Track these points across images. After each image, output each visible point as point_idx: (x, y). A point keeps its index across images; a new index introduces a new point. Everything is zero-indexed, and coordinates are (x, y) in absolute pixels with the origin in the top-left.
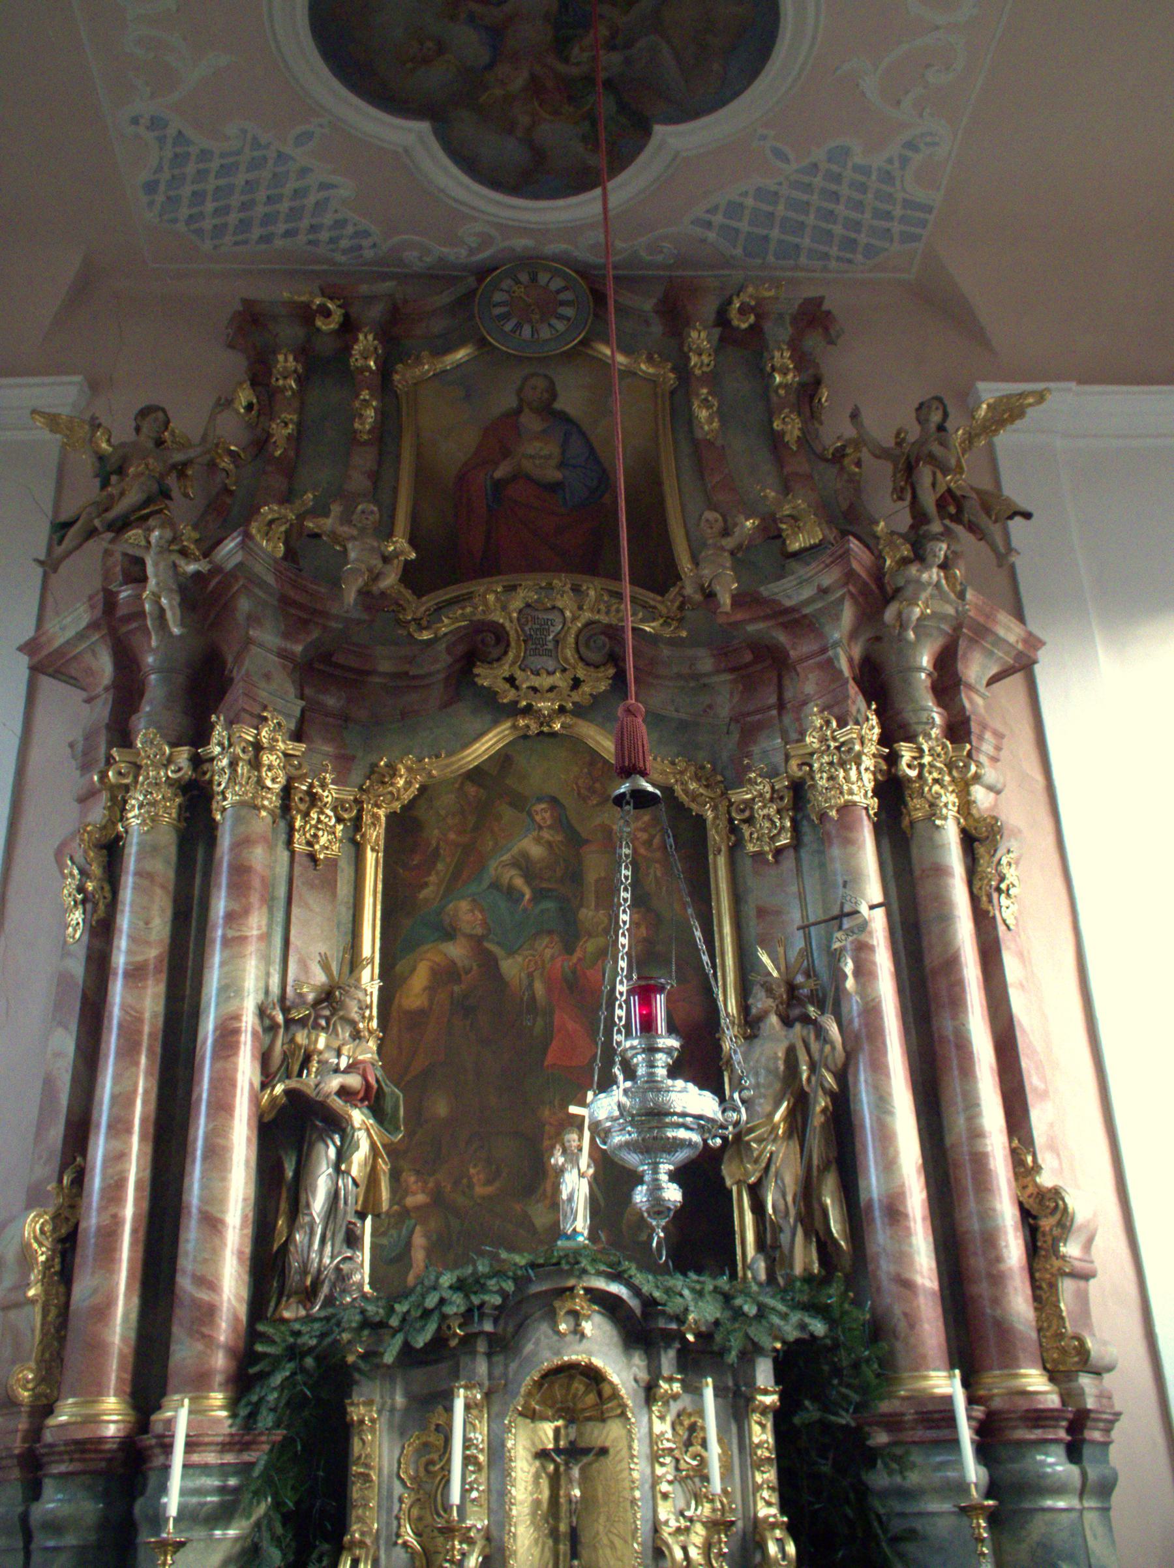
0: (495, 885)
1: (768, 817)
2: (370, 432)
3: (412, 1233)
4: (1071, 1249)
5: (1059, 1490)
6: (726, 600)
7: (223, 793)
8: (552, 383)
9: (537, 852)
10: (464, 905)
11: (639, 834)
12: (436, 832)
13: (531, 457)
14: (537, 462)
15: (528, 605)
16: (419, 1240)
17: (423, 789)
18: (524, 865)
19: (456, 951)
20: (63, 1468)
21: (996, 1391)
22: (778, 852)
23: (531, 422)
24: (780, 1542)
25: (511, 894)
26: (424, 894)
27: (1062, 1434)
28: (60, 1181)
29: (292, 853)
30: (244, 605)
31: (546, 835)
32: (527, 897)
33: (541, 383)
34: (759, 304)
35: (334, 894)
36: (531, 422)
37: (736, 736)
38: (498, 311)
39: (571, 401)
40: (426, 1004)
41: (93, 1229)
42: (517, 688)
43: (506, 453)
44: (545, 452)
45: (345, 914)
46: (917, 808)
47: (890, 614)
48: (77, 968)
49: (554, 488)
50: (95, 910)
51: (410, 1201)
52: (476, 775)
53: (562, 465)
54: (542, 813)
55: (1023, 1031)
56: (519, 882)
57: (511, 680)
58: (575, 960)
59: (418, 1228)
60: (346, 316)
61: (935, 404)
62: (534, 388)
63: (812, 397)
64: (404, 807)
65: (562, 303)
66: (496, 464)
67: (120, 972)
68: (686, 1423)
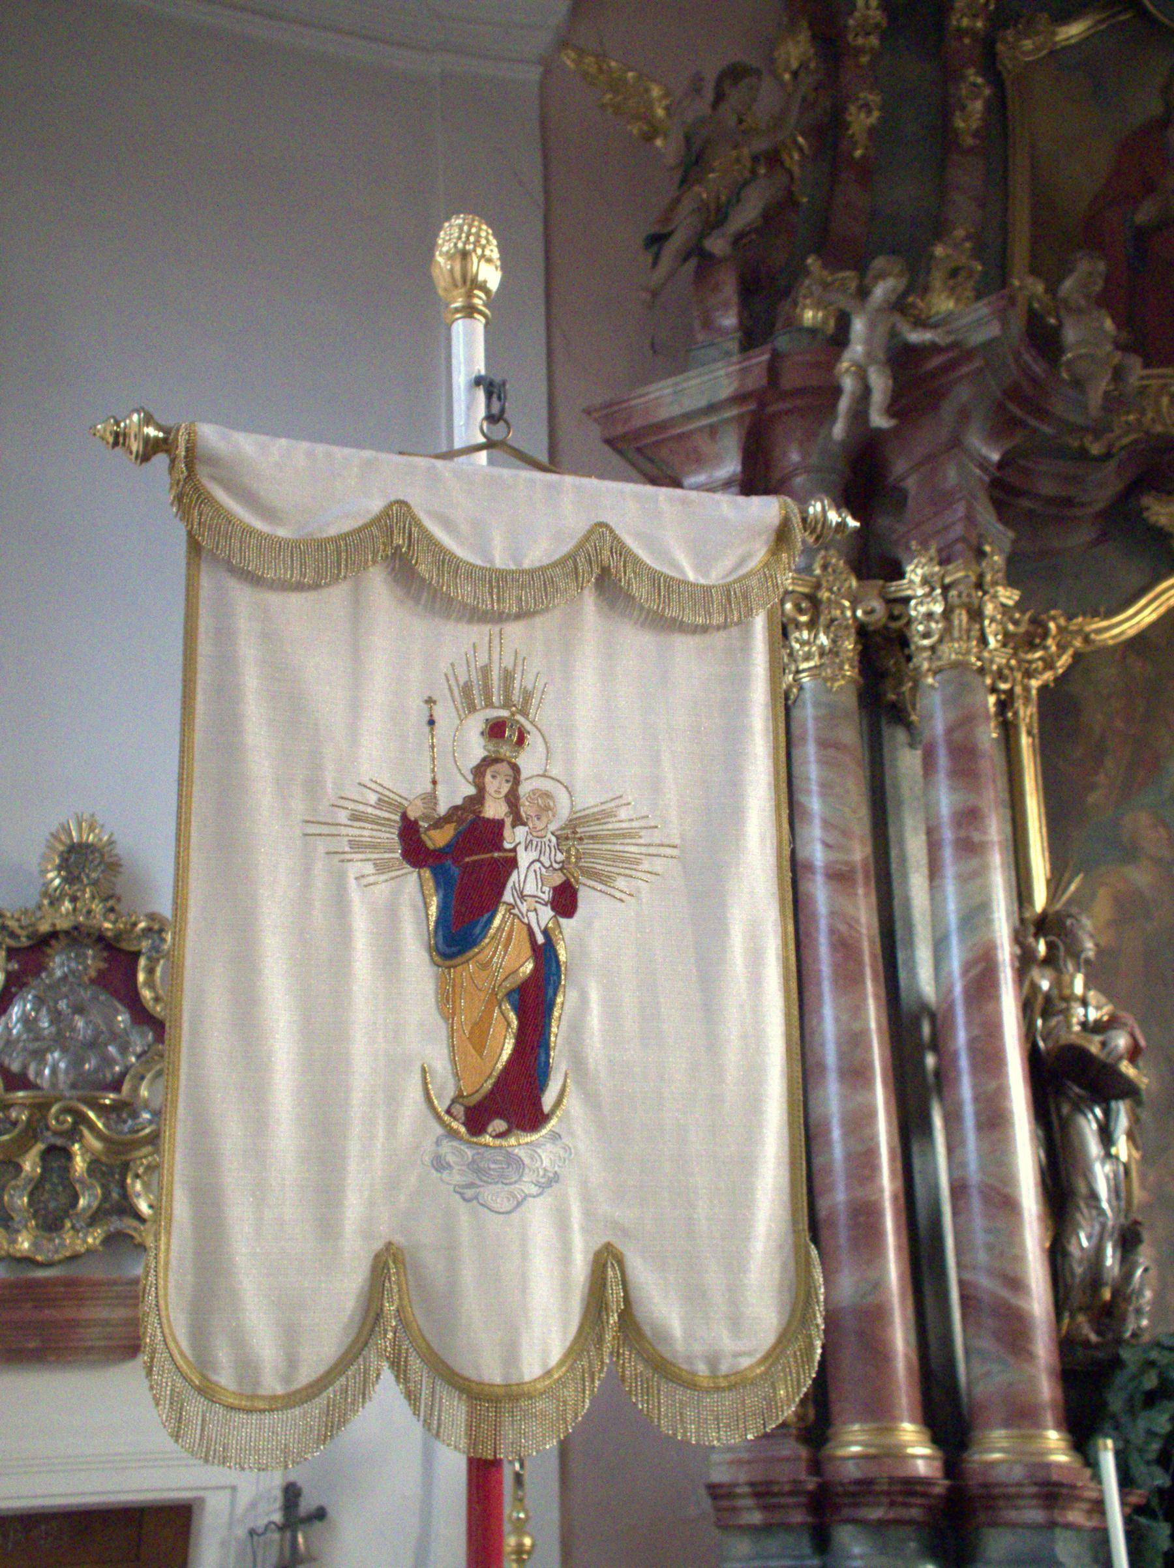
2: (975, 135)
10: (1144, 818)
12: (1099, 717)
20: (876, 1514)
26: (1092, 798)
30: (963, 393)
41: (841, 1208)
43: (1149, 187)
64: (1057, 680)
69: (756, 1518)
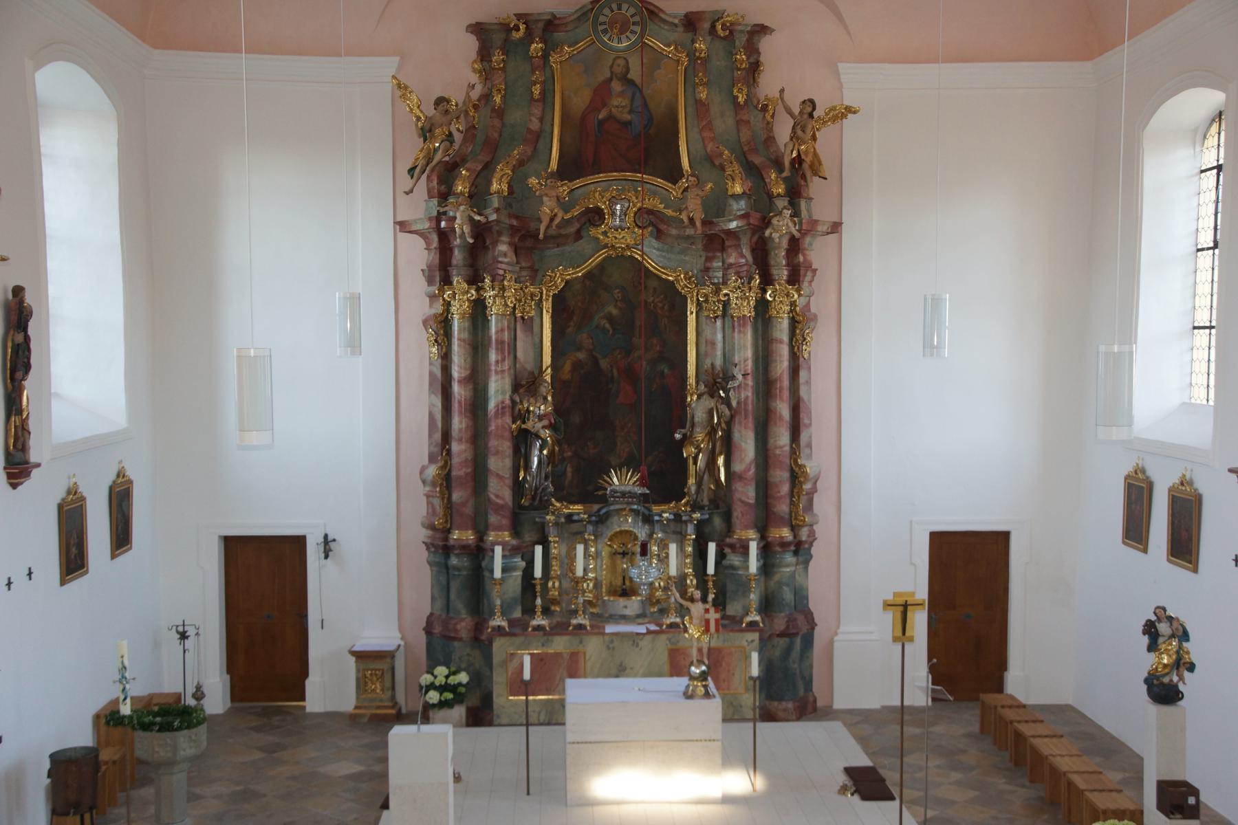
0: (597, 327)
1: (714, 302)
3: (566, 466)
4: (807, 486)
5: (788, 566)
6: (698, 224)
9: (615, 312)
10: (585, 336)
11: (659, 304)
13: (617, 107)
14: (620, 109)
15: (613, 197)
16: (569, 469)
17: (567, 282)
18: (610, 318)
21: (771, 535)
23: (616, 86)
24: (691, 581)
26: (570, 330)
27: (793, 548)
28: (442, 455)
29: (516, 318)
31: (619, 304)
32: (611, 333)
34: (732, 24)
35: (532, 333)
36: (616, 86)
37: (703, 259)
38: (601, 28)
39: (634, 74)
40: (570, 378)
42: (608, 237)
43: (605, 105)
44: (624, 104)
45: (537, 340)
47: (767, 233)
48: (438, 372)
49: (627, 124)
50: (442, 349)
52: (589, 275)
53: (630, 112)
55: (803, 400)
56: (607, 326)
57: (605, 233)
58: (629, 360)
59: (569, 465)
60: (527, 28)
61: (809, 103)
62: (619, 66)
63: (754, 71)
65: (634, 24)
66: (599, 111)
67: (456, 380)
68: (663, 543)
69: (433, 549)
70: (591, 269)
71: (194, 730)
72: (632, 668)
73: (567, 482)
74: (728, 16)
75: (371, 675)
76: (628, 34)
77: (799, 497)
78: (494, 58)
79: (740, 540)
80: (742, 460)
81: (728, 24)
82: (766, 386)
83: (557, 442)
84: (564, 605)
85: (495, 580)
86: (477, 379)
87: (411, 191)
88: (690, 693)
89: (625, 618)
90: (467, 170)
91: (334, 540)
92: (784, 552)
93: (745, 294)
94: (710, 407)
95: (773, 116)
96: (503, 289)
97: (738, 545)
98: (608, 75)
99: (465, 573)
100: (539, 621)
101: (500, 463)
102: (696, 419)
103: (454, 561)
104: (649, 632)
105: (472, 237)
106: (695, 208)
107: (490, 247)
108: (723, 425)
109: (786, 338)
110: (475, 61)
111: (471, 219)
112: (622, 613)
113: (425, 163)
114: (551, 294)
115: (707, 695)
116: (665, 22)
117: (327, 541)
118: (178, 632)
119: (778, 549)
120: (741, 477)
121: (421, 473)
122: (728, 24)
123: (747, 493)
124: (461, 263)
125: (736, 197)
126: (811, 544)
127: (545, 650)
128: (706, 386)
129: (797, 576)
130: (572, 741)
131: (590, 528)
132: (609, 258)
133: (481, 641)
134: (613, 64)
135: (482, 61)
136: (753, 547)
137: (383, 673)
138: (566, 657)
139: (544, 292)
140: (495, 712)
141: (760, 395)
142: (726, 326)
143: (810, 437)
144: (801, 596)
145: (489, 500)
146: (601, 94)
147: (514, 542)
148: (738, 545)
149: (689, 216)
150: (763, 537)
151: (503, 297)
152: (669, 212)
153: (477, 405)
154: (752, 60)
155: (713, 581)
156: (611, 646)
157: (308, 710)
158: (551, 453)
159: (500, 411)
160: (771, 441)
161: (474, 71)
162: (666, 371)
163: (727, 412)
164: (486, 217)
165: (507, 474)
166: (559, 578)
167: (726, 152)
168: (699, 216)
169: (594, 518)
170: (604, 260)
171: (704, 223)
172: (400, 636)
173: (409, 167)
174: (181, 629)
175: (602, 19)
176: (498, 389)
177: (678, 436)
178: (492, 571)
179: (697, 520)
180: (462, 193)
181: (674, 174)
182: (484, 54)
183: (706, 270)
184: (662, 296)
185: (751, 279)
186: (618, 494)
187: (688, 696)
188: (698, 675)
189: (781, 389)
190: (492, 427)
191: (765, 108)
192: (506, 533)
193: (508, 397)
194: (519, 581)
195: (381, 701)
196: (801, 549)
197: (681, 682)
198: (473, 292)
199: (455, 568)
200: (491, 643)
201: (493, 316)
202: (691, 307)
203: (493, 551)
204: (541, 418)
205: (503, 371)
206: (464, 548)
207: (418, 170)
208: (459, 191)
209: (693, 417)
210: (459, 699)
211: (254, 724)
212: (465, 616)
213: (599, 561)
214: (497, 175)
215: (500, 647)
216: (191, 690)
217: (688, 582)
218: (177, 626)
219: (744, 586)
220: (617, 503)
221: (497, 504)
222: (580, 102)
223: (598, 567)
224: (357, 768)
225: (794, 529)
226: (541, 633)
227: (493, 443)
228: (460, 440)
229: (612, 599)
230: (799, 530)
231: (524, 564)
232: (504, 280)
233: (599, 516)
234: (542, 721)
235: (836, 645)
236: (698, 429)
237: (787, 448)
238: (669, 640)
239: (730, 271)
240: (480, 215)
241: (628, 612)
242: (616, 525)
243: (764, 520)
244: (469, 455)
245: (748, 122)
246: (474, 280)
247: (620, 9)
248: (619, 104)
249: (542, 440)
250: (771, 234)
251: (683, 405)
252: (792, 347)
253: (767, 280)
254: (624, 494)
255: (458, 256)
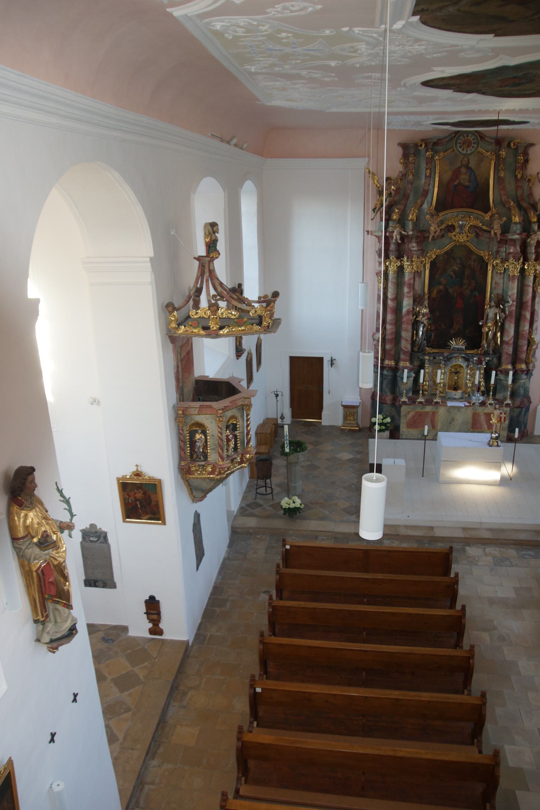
1: (500, 266)
4: (534, 347)
5: (523, 380)
7: (406, 269)
8: (469, 160)
9: (456, 269)
13: (463, 179)
16: (433, 335)
17: (437, 256)
18: (454, 271)
19: (441, 287)
22: (500, 273)
23: (463, 170)
25: (451, 277)
26: (436, 276)
27: (526, 372)
31: (459, 266)
33: (466, 159)
34: (518, 143)
36: (463, 170)
37: (497, 246)
39: (472, 164)
43: (457, 178)
45: (422, 280)
46: (527, 273)
49: (467, 187)
51: (432, 328)
52: (446, 253)
53: (469, 181)
54: (458, 261)
56: (453, 275)
57: (455, 236)
59: (433, 333)
62: (465, 161)
64: (433, 260)
70: (448, 250)
71: (305, 452)
72: (457, 420)
73: (432, 340)
74: (517, 139)
75: (349, 414)
76: (471, 148)
77: (530, 351)
78: (410, 159)
79: (505, 369)
80: (508, 336)
81: (516, 143)
82: (521, 304)
83: (430, 324)
84: (429, 392)
85: (404, 383)
86: (398, 300)
87: (374, 218)
88: (491, 444)
89: (455, 399)
90: (397, 209)
91: (335, 360)
92: (522, 374)
93: (516, 266)
94: (496, 312)
95: (532, 184)
96: (412, 262)
97: (504, 371)
98: (459, 165)
99: (390, 378)
100: (421, 400)
101: (406, 335)
102: (489, 317)
103: (385, 372)
104: (465, 406)
105: (400, 240)
106: (497, 228)
107: (407, 243)
108: (501, 320)
109: (531, 284)
110: (401, 159)
111: (401, 233)
112: (453, 397)
113: (380, 206)
114: (430, 260)
115: (498, 446)
116: (487, 141)
117: (332, 360)
118: (275, 394)
119: (520, 373)
120: (507, 343)
121: (373, 336)
122: (516, 143)
123: (509, 349)
124: (394, 249)
125: (516, 223)
126: (533, 370)
127: (422, 410)
128: (495, 303)
129: (526, 384)
130: (443, 460)
131: (443, 362)
132: (455, 246)
133: (396, 405)
134: (462, 160)
135: (404, 159)
136: (511, 373)
137: (354, 414)
138: (431, 414)
139: (427, 260)
140: (401, 434)
141: (518, 307)
142: (505, 277)
143: (537, 326)
144: (526, 390)
145: (401, 349)
146: (456, 174)
147: (411, 366)
148: (504, 371)
149: (494, 232)
150: (514, 368)
151: (412, 265)
152: (484, 228)
153: (398, 310)
154: (525, 158)
155: (493, 387)
156: (449, 411)
157: (323, 424)
158: (427, 329)
159: (408, 312)
160: (521, 328)
161: (401, 163)
162: (477, 294)
163: (504, 316)
164: (408, 233)
165: (409, 339)
166: (428, 381)
167: (512, 202)
168: (499, 232)
169: (445, 359)
170: (453, 246)
171: (501, 234)
172: (360, 398)
173: (373, 208)
174: (276, 393)
175: (459, 141)
176: (407, 304)
177: (481, 323)
178: (402, 378)
179: (488, 361)
180: (395, 220)
181: (486, 209)
182: (405, 156)
183: (498, 252)
184: (477, 263)
185: (519, 259)
186: (456, 349)
187: (490, 445)
188: (494, 438)
189: (527, 306)
190: (404, 319)
191: (529, 180)
192: (408, 363)
193: (411, 307)
194: (412, 381)
195: (353, 424)
196: (528, 372)
197: (485, 437)
198: (399, 263)
199: (386, 375)
200: (400, 406)
201: (407, 273)
202: (490, 268)
203: (403, 371)
204: (424, 315)
205: (410, 296)
206: (390, 368)
207: (377, 209)
208: (394, 218)
209: (488, 316)
210: (386, 429)
211: (304, 430)
212: (389, 395)
213: (445, 375)
214: (412, 213)
215: (404, 409)
216: (279, 416)
217: (481, 384)
218: (275, 392)
219: (505, 387)
220: (456, 353)
221: (405, 351)
222: (447, 177)
223: (445, 378)
224: (351, 456)
225: (527, 364)
226: (421, 405)
227: (404, 326)
228: (390, 324)
229: (449, 391)
230: (529, 365)
231: (414, 375)
232: (412, 258)
233: (448, 358)
234: (419, 438)
235: (538, 410)
236: (489, 321)
237: (528, 331)
238: (473, 409)
239: (510, 255)
240: (405, 231)
241: (456, 397)
242: (454, 362)
243: (515, 360)
244: (394, 330)
245: (521, 187)
246: (399, 257)
247: (468, 136)
248: (464, 178)
249: (424, 324)
250: (530, 241)
251: (483, 310)
252: (533, 288)
253: (526, 260)
254: (458, 349)
255: (392, 247)
